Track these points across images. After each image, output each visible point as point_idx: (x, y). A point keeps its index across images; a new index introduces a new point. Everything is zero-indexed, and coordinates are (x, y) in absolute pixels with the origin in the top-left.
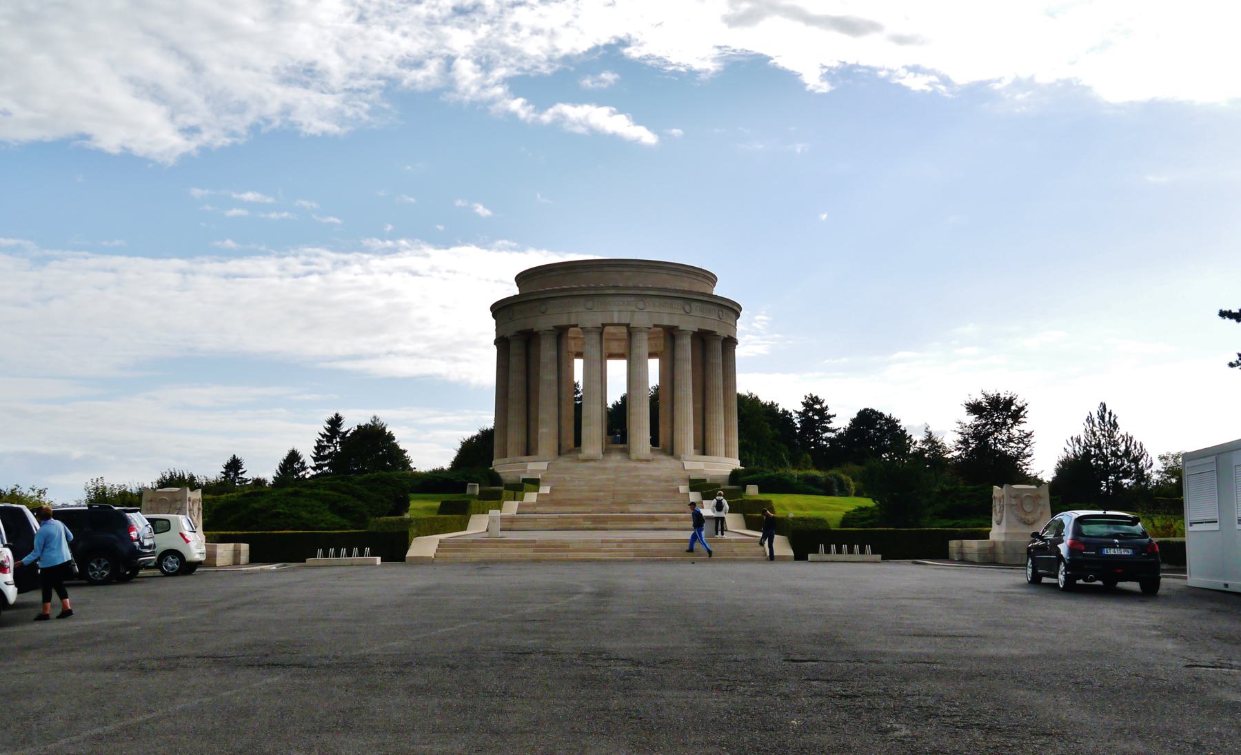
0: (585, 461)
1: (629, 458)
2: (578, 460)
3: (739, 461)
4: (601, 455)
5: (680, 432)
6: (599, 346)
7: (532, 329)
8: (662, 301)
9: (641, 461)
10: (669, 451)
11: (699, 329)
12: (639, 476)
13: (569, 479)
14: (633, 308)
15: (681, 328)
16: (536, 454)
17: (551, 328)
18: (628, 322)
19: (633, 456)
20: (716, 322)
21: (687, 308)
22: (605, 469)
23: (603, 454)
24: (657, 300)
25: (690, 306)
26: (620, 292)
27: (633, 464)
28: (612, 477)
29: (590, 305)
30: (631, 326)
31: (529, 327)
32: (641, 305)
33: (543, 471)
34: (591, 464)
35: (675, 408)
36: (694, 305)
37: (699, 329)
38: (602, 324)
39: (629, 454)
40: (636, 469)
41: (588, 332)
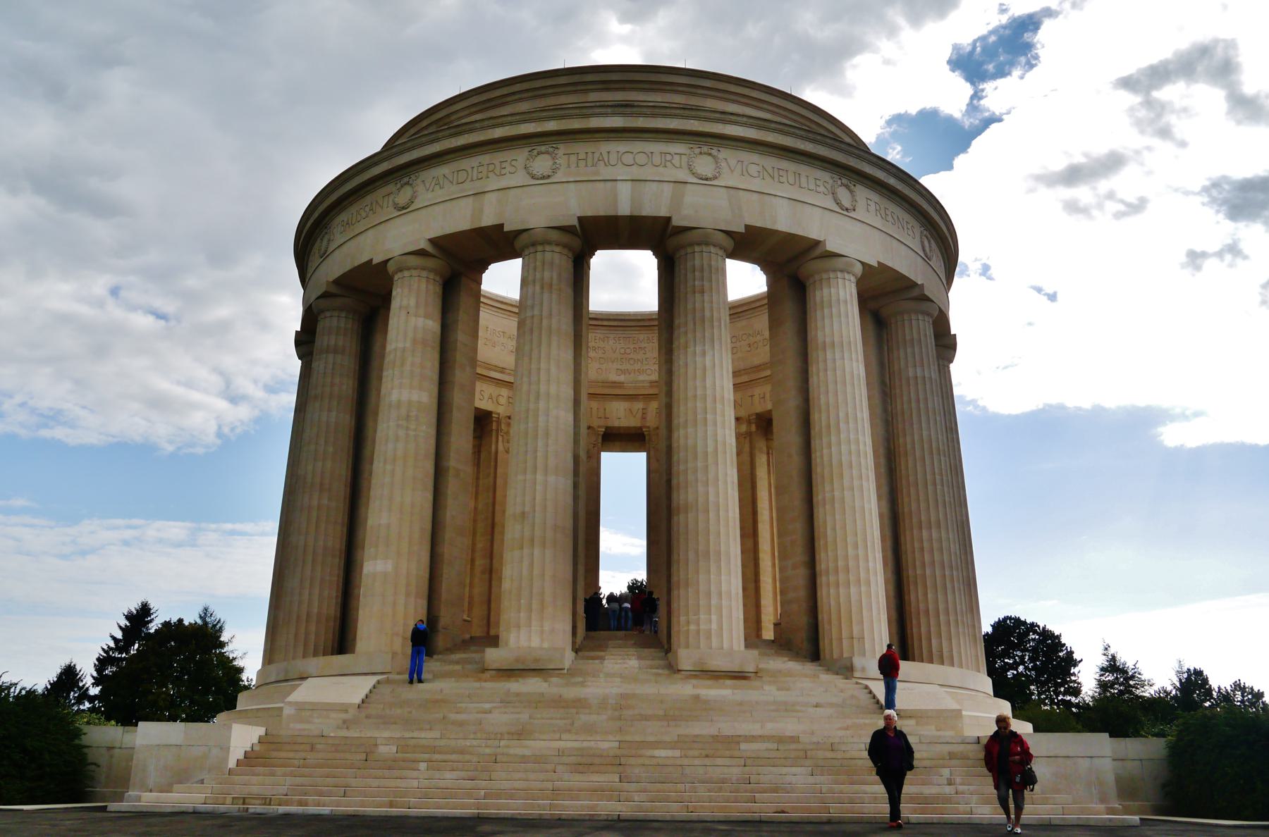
0: (508, 673)
1: (673, 669)
2: (484, 670)
3: (989, 681)
4: (569, 655)
5: (842, 577)
6: (569, 292)
7: (372, 260)
8: (771, 162)
9: (716, 675)
10: (801, 637)
11: (879, 263)
12: (732, 742)
13: (386, 750)
14: (683, 175)
15: (831, 246)
16: (354, 653)
17: (423, 245)
18: (663, 213)
19: (686, 657)
20: (919, 259)
21: (846, 199)
22: (580, 704)
23: (576, 650)
24: (755, 157)
25: (851, 192)
26: (641, 122)
27: (684, 689)
28: (607, 745)
29: (542, 164)
30: (676, 222)
31: (364, 259)
32: (704, 165)
33: (344, 708)
34: (533, 685)
35: (818, 498)
36: (862, 193)
37: (879, 263)
38: (580, 218)
39: (668, 650)
40: (700, 707)
41: (534, 244)
